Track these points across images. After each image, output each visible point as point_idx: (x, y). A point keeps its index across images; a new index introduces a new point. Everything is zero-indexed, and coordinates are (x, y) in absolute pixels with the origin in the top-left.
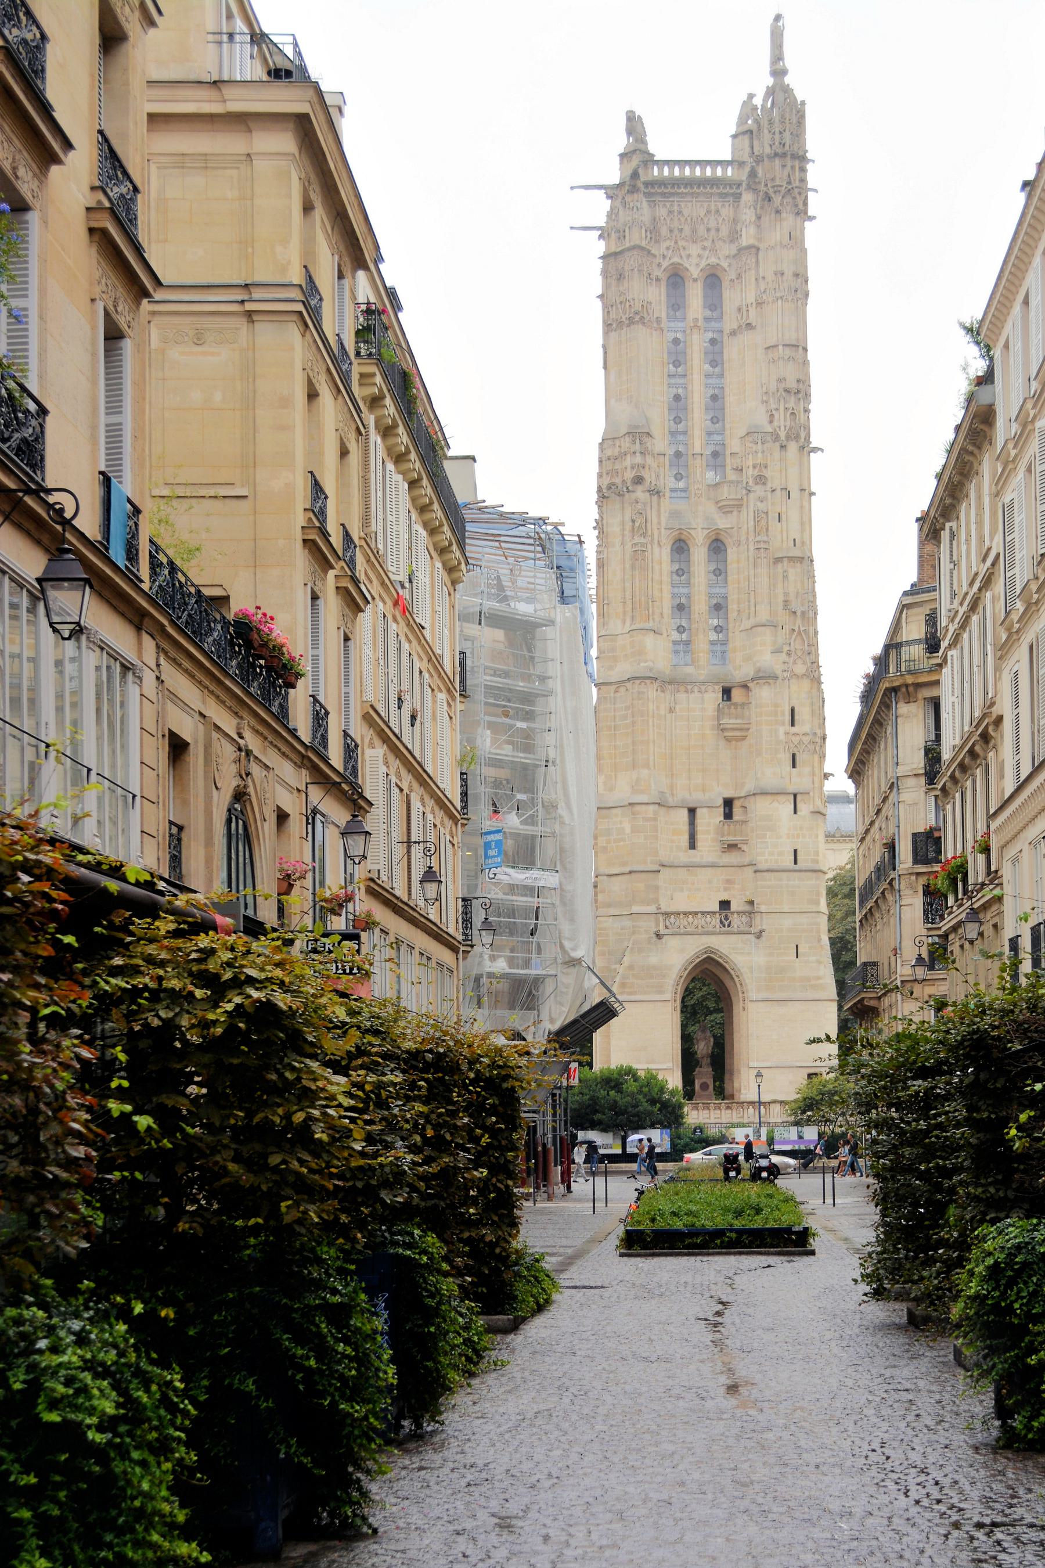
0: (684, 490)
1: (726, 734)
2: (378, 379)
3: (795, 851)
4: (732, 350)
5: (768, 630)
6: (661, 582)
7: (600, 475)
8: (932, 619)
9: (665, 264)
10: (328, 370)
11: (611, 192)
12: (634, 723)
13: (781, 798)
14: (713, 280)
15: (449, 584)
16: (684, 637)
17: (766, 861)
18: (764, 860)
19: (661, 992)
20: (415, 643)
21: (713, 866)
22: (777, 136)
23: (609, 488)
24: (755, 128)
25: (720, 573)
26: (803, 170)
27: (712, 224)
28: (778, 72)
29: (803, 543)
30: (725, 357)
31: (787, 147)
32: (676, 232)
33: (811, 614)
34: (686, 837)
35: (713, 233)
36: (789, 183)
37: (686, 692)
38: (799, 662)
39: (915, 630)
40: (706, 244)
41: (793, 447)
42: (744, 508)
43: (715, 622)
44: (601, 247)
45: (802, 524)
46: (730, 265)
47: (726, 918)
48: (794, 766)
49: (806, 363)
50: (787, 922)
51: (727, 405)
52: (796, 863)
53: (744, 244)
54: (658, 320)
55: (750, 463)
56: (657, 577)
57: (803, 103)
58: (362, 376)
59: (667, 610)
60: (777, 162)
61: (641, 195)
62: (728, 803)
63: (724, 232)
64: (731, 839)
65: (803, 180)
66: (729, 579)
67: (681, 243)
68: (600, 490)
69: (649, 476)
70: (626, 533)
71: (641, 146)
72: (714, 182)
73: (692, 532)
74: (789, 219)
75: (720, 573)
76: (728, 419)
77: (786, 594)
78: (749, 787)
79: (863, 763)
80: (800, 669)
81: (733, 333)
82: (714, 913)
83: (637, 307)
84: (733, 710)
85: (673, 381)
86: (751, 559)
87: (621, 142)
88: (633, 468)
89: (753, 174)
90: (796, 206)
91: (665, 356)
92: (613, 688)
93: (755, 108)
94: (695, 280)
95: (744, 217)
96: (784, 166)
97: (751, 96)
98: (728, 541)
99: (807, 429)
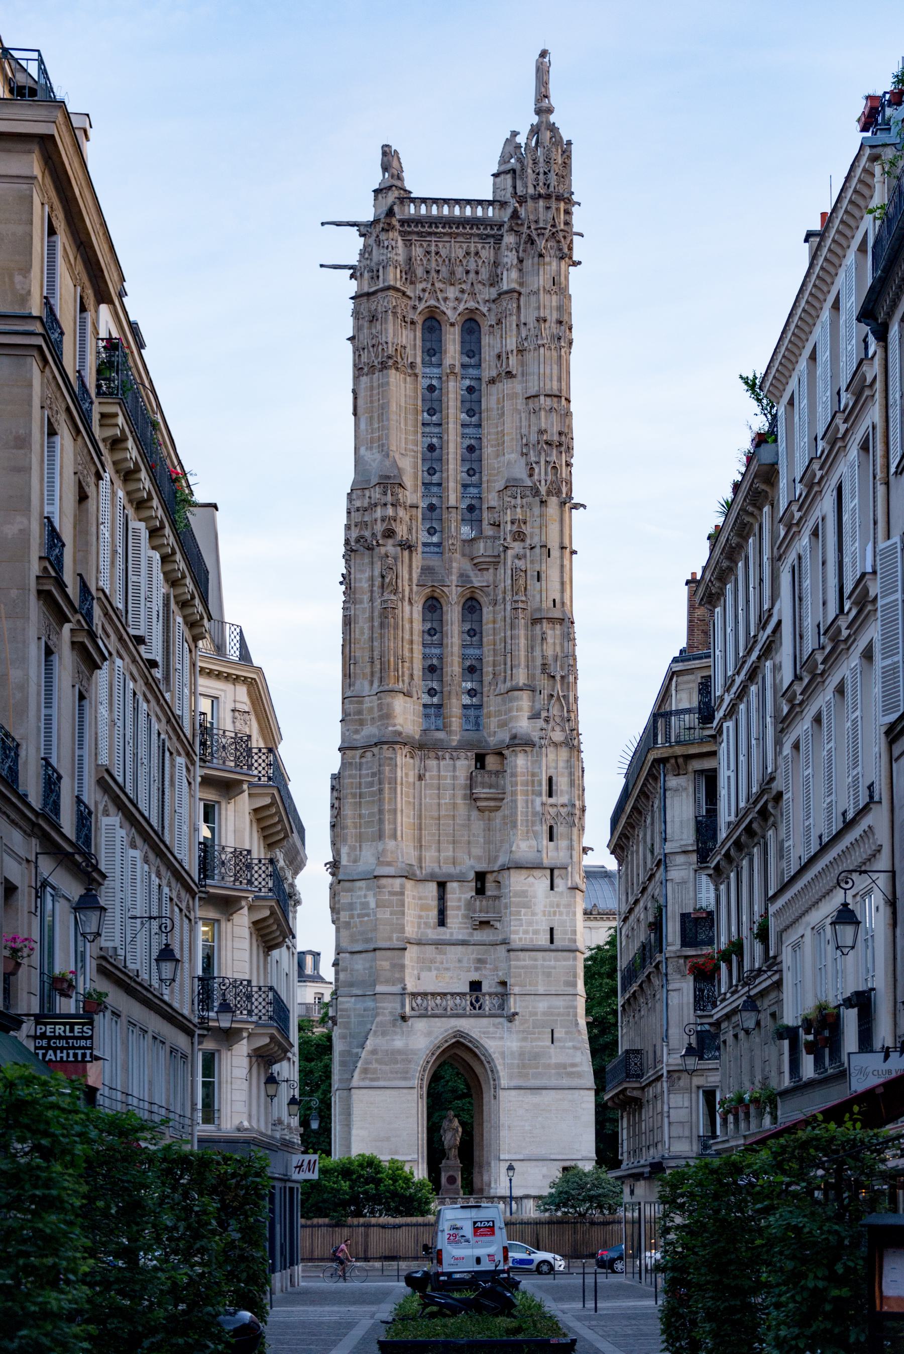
0: (439, 545)
1: (480, 804)
2: (121, 420)
3: (552, 929)
4: (490, 399)
5: (525, 695)
6: (411, 642)
7: (348, 527)
8: (705, 687)
9: (421, 307)
10: (68, 409)
11: (364, 229)
12: (381, 791)
13: (538, 873)
14: (471, 326)
15: (190, 640)
16: (435, 700)
17: (520, 939)
18: (518, 938)
19: (405, 1079)
20: (153, 703)
21: (464, 943)
22: (541, 176)
23: (357, 541)
24: (518, 167)
25: (474, 633)
26: (568, 213)
27: (472, 267)
28: (543, 110)
29: (563, 604)
30: (484, 407)
31: (551, 189)
32: (433, 274)
33: (571, 679)
34: (435, 912)
35: (472, 275)
36: (554, 226)
37: (437, 758)
38: (558, 728)
39: (686, 698)
40: (464, 286)
41: (553, 501)
42: (501, 565)
43: (469, 685)
44: (352, 287)
45: (562, 583)
46: (489, 310)
47: (477, 1001)
48: (551, 839)
49: (568, 414)
50: (542, 1005)
51: (485, 456)
52: (552, 942)
53: (505, 288)
54: (412, 365)
55: (509, 519)
56: (407, 636)
57: (569, 143)
58: (103, 416)
59: (418, 672)
60: (541, 203)
61: (396, 234)
62: (481, 877)
63: (484, 275)
64: (484, 916)
65: (568, 223)
66: (485, 640)
67: (439, 285)
68: (347, 543)
69: (401, 531)
70: (375, 589)
71: (398, 183)
72: (474, 222)
73: (445, 589)
74: (553, 265)
75: (474, 633)
76: (485, 472)
77: (544, 657)
78: (502, 860)
79: (628, 838)
80: (558, 736)
81: (492, 381)
82: (464, 994)
83: (391, 351)
84: (487, 779)
85: (427, 429)
86: (508, 621)
87: (376, 178)
88: (383, 520)
89: (515, 215)
90: (560, 250)
91: (420, 403)
92: (358, 753)
93: (519, 146)
94: (452, 325)
95: (505, 260)
96: (548, 208)
97: (515, 134)
98: (484, 600)
99: (569, 483)
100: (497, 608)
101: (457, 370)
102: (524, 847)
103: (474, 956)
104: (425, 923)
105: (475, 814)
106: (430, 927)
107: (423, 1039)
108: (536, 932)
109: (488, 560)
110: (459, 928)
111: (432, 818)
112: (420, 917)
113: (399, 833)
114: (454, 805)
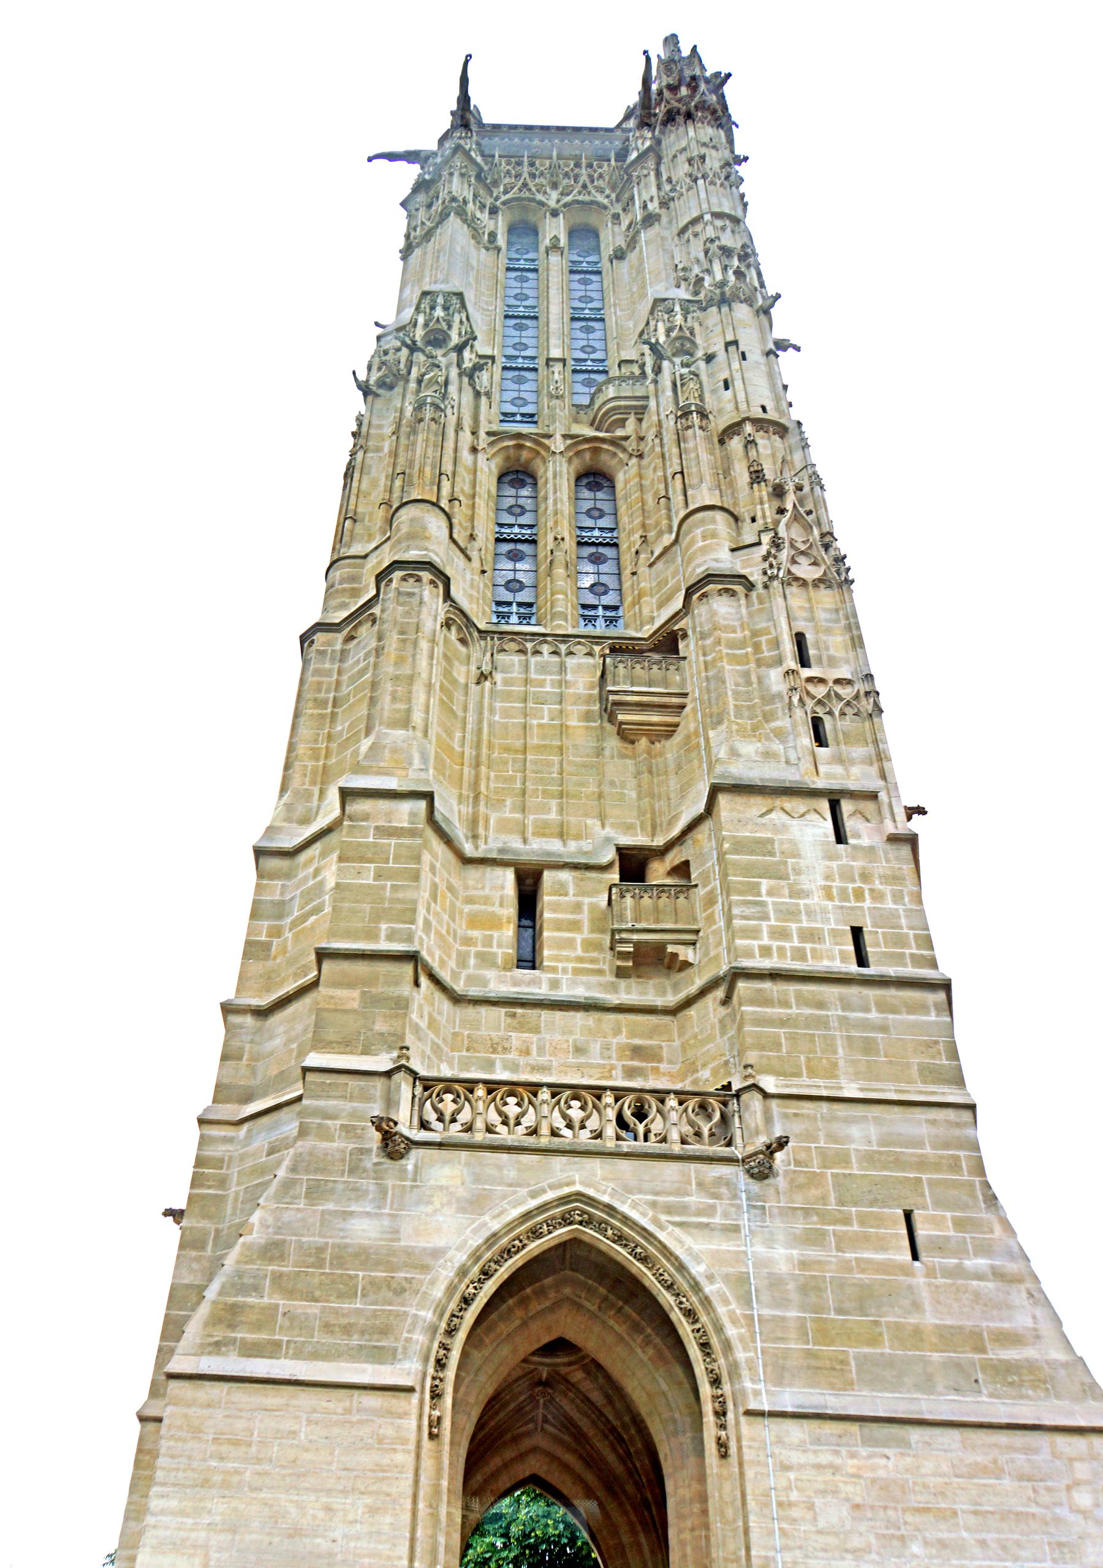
3: (857, 933)
19: (381, 1356)
37: (523, 651)
48: (820, 739)
50: (862, 1133)
54: (493, 236)
100: (645, 462)
101: (563, 242)
102: (748, 761)
103: (623, 1039)
104: (480, 955)
105: (613, 743)
106: (494, 965)
107: (455, 1219)
108: (810, 935)
109: (623, 403)
110: (577, 972)
111: (507, 749)
112: (468, 941)
113: (417, 717)
114: (563, 729)
